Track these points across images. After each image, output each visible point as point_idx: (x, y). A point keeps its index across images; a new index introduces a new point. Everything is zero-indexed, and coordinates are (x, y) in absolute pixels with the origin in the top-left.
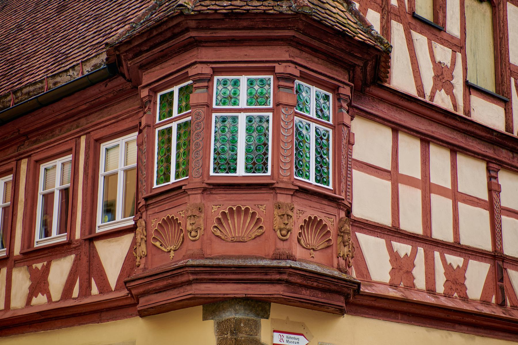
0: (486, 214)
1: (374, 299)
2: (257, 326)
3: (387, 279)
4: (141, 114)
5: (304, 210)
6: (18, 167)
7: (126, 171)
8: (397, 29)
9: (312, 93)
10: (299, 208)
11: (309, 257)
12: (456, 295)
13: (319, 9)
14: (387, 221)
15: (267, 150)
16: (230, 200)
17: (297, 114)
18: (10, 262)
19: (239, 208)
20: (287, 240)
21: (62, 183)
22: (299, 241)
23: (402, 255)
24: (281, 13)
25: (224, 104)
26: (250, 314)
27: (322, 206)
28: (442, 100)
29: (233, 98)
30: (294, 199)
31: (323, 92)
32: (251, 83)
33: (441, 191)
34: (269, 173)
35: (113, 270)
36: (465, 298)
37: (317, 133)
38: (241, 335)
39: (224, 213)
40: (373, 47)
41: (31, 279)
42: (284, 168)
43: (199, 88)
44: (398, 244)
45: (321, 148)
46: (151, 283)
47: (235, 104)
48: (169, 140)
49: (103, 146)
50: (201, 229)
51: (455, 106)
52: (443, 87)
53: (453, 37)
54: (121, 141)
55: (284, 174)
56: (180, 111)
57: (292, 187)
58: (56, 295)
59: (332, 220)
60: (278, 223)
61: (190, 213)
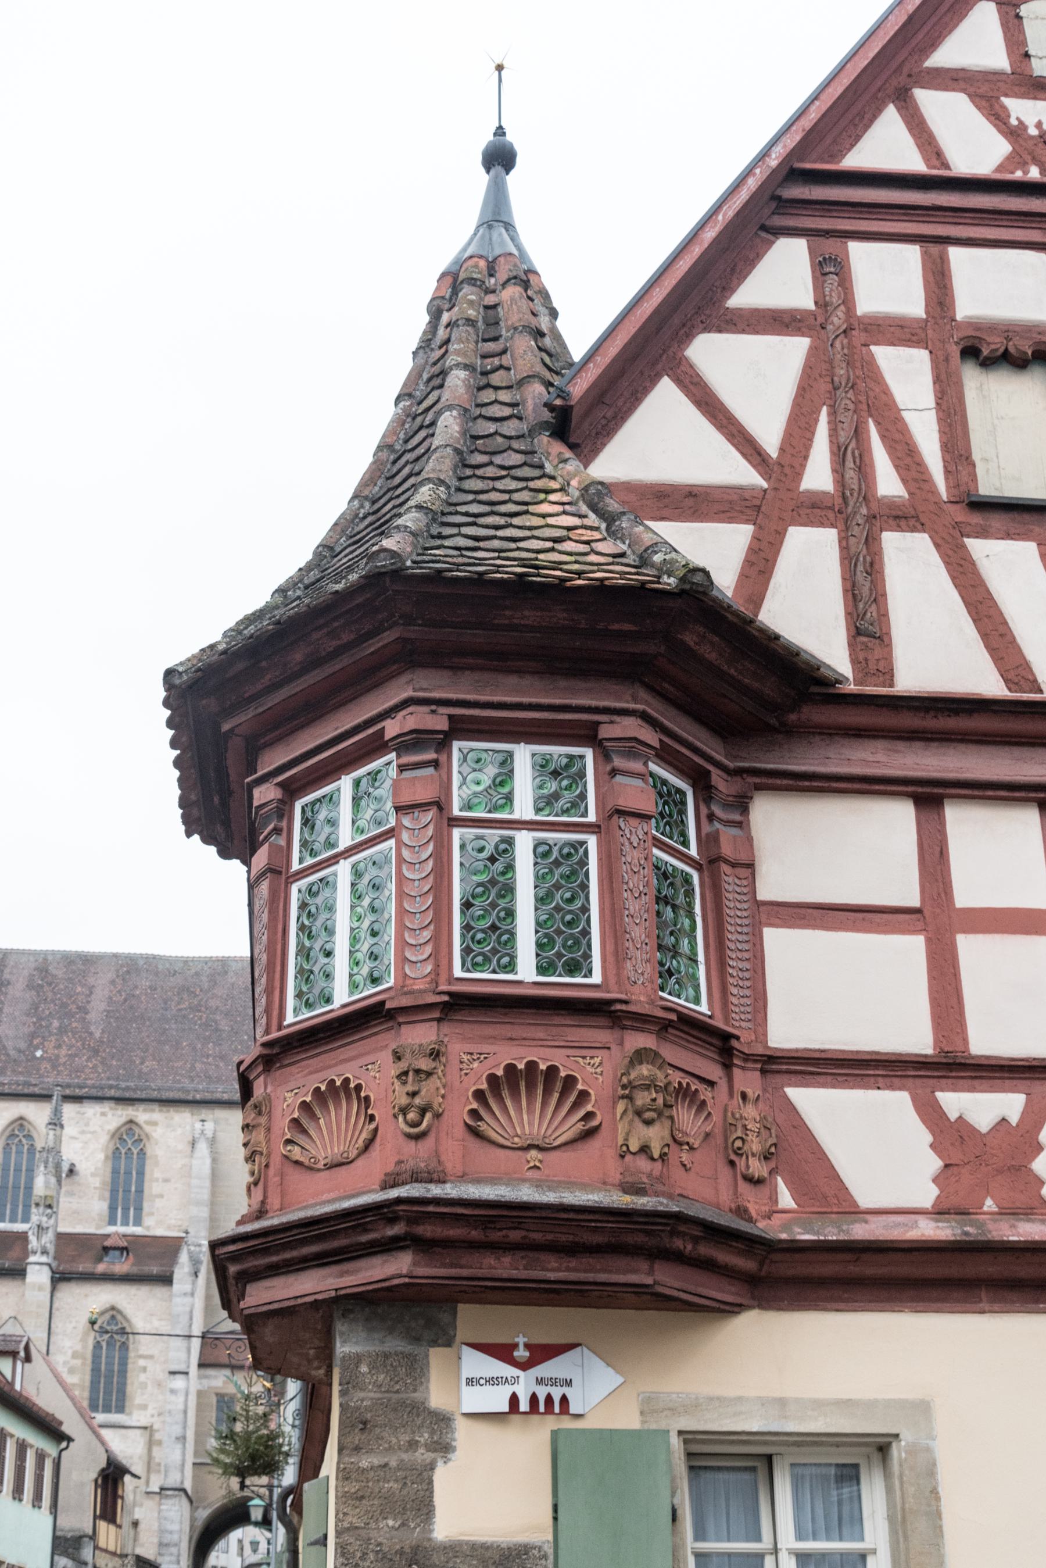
1: (848, 1256)
2: (415, 1370)
16: (317, 1071)
26: (389, 1338)
27: (554, 1030)
30: (446, 1028)
31: (558, 751)
38: (362, 1395)
42: (413, 959)
50: (262, 1154)
59: (597, 1060)
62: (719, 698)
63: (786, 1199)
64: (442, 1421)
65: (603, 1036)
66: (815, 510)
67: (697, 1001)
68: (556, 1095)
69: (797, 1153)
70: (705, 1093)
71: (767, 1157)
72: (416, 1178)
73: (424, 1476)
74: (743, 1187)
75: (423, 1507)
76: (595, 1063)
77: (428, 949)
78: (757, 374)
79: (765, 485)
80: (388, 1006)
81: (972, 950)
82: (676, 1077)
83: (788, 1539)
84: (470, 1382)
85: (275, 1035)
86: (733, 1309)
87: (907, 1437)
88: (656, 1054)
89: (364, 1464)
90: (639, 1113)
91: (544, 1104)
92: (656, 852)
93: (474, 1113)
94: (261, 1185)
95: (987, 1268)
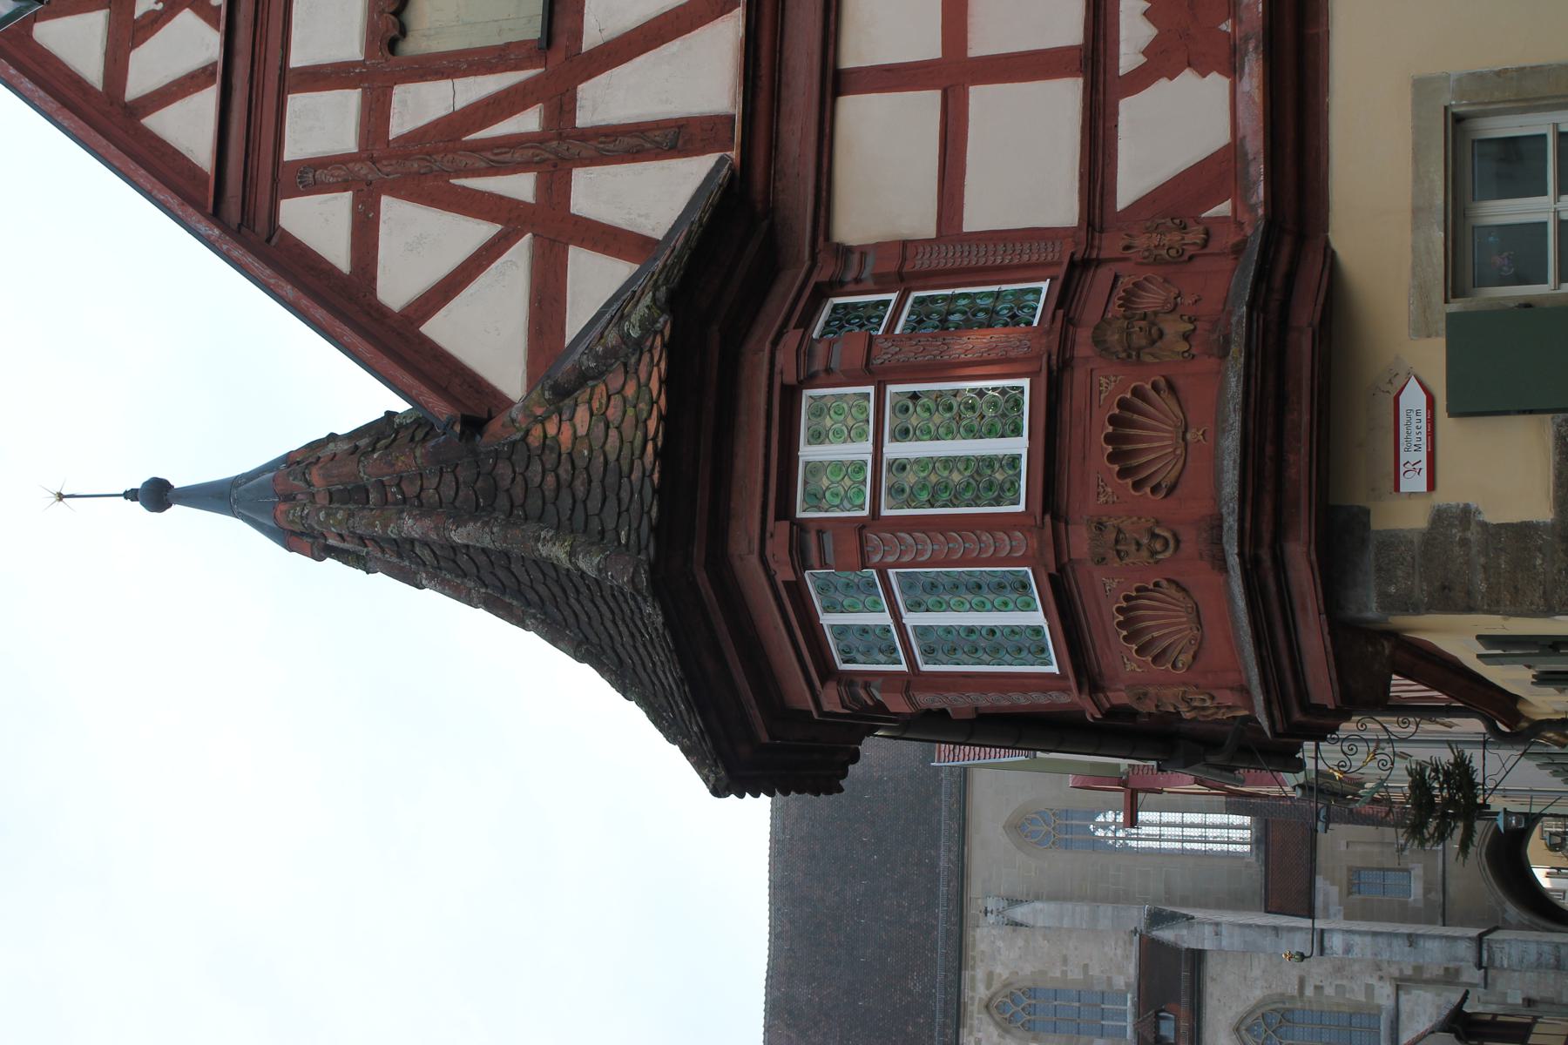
2: (1392, 541)
3: (1217, 84)
20: (1175, 536)
22: (1172, 489)
57: (1048, 531)
59: (1103, 380)
62: (748, 275)
63: (1224, 208)
65: (1079, 375)
66: (555, 188)
67: (1038, 291)
68: (1135, 416)
70: (1126, 282)
71: (1183, 227)
72: (1217, 541)
74: (1213, 247)
75: (1523, 531)
76: (1102, 386)
77: (1000, 535)
78: (417, 245)
79: (529, 236)
80: (1053, 571)
81: (981, 44)
82: (1115, 309)
83: (1547, 201)
85: (1072, 682)
86: (1330, 257)
88: (1096, 328)
89: (1483, 587)
90: (1153, 342)
91: (1143, 427)
92: (898, 331)
93: (1154, 490)
94: (1214, 693)
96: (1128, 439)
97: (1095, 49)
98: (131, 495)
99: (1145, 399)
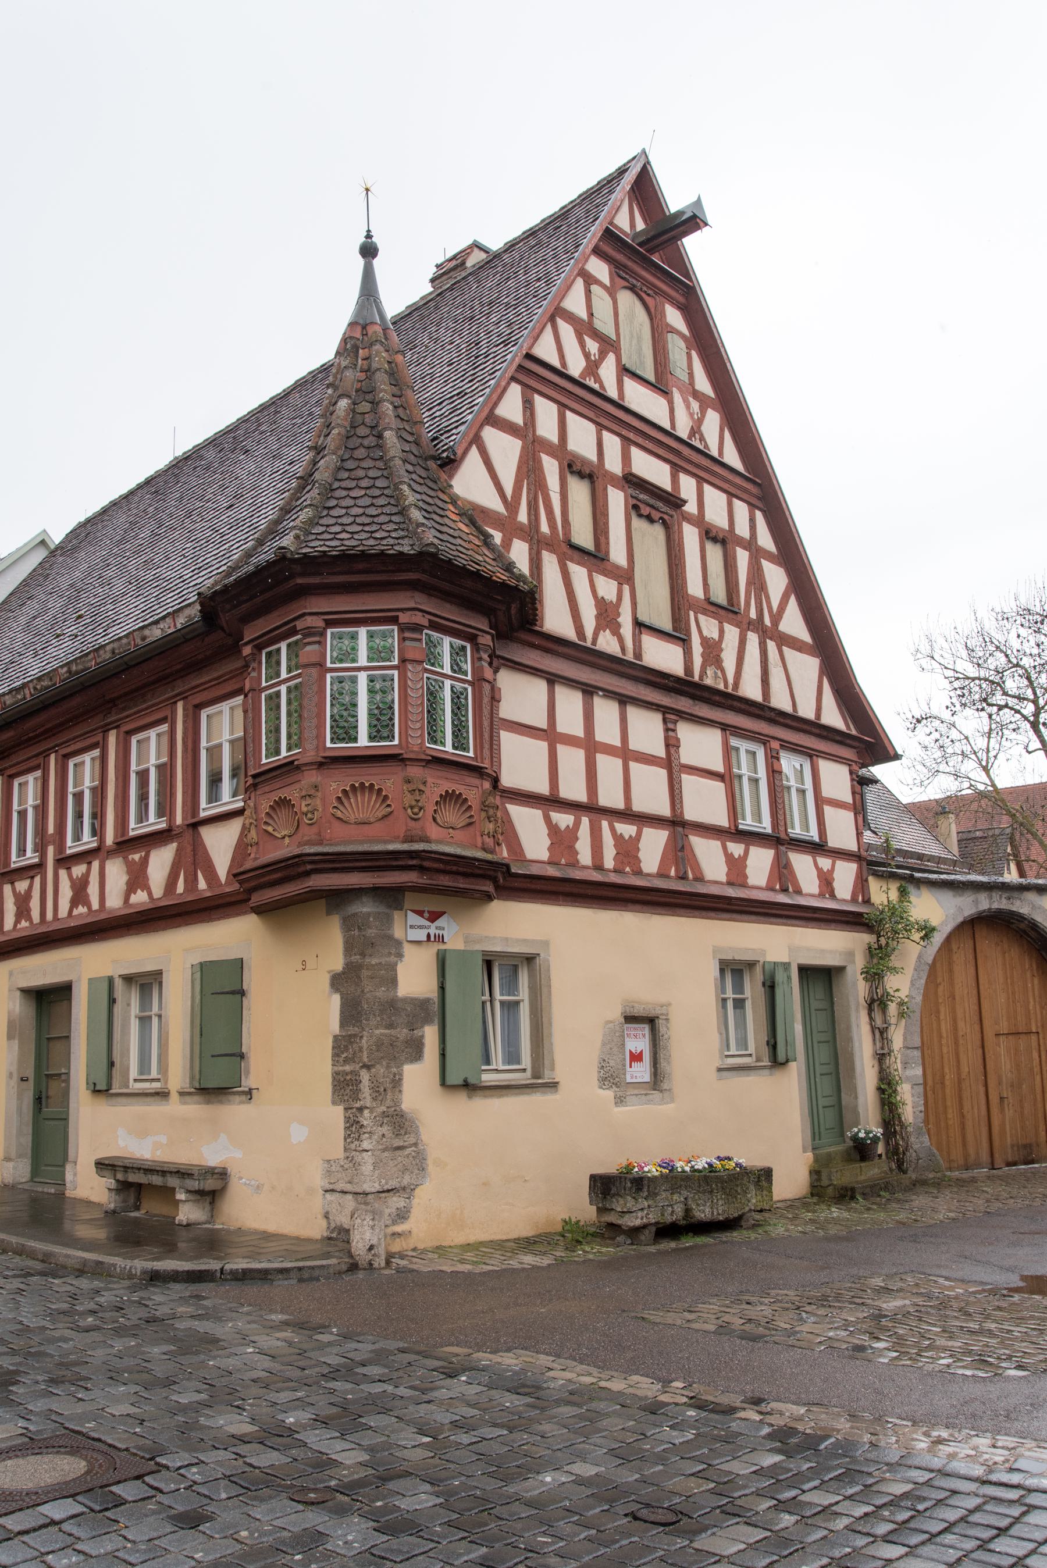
0: (663, 773)
2: (389, 920)
3: (545, 856)
4: (245, 674)
5: (438, 783)
6: (105, 739)
7: (232, 742)
8: (550, 563)
9: (447, 643)
10: (433, 780)
11: (448, 838)
12: (628, 869)
13: (449, 545)
14: (544, 789)
15: (393, 714)
17: (427, 670)
18: (103, 853)
19: (362, 784)
21: (158, 758)
22: (434, 819)
23: (563, 826)
24: (401, 553)
25: (341, 661)
28: (607, 643)
29: (351, 654)
30: (427, 771)
31: (459, 642)
32: (371, 636)
33: (609, 750)
34: (396, 742)
35: (222, 862)
36: (638, 872)
37: (452, 690)
38: (370, 931)
39: (345, 791)
40: (516, 588)
41: (128, 872)
43: (309, 643)
44: (558, 815)
45: (459, 708)
46: (263, 875)
47: (354, 661)
48: (278, 707)
49: (204, 714)
51: (623, 649)
52: (607, 626)
53: (618, 567)
54: (225, 706)
55: (414, 742)
56: (289, 671)
57: (424, 757)
58: (158, 891)
60: (409, 799)
61: (304, 793)
64: (399, 943)
65: (477, 782)
69: (508, 833)
73: (392, 968)
75: (393, 982)
84: (411, 927)
86: (489, 898)
87: (542, 955)
95: (567, 888)
96: (450, 800)
97: (558, 802)
98: (369, 236)
99: (466, 810)
